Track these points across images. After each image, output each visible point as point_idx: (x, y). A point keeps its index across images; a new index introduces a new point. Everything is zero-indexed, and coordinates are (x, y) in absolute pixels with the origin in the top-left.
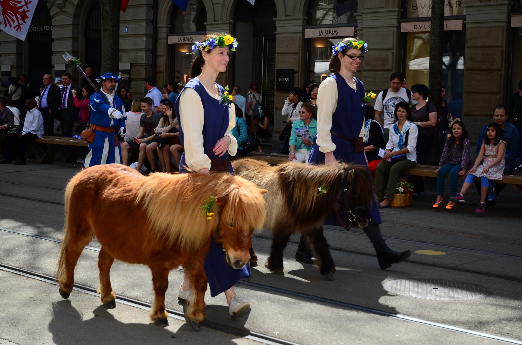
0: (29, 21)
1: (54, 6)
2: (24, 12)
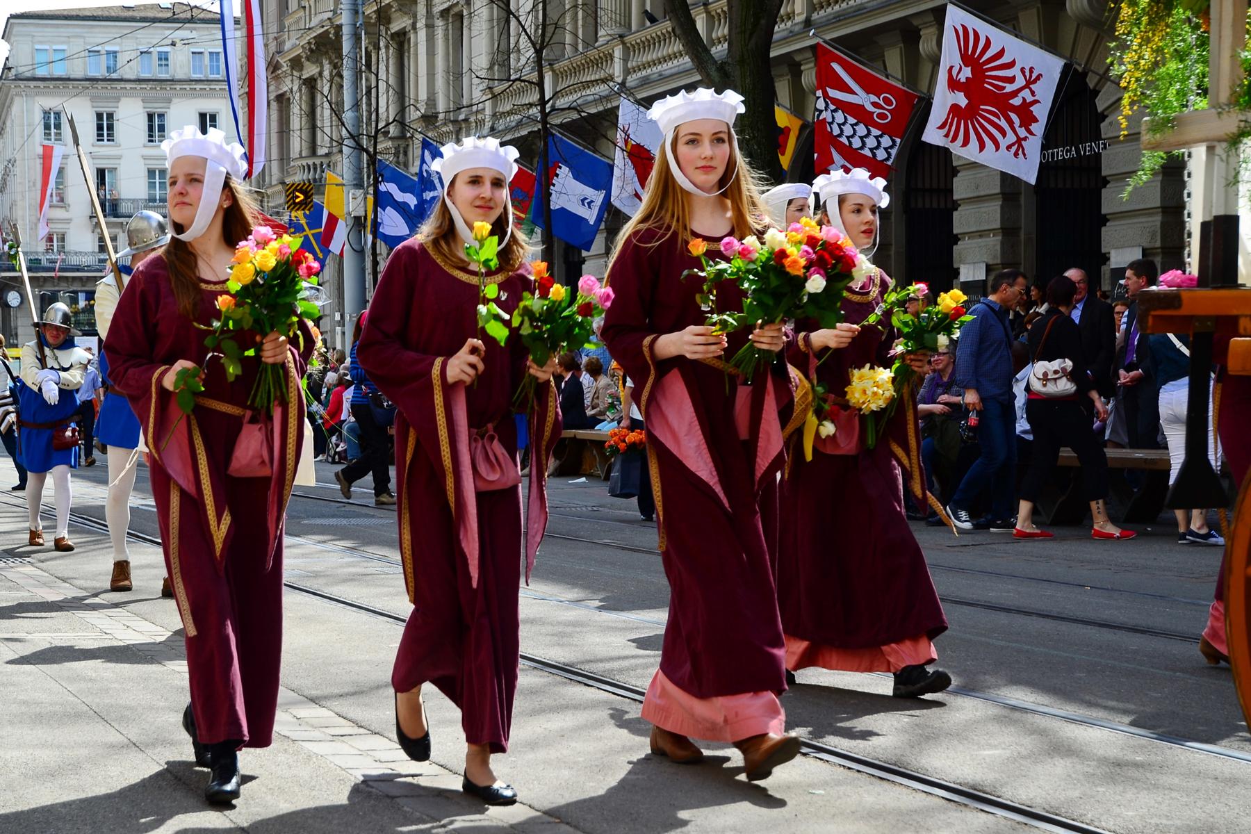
0: (1039, 128)
1: (1109, 83)
2: (1026, 105)
